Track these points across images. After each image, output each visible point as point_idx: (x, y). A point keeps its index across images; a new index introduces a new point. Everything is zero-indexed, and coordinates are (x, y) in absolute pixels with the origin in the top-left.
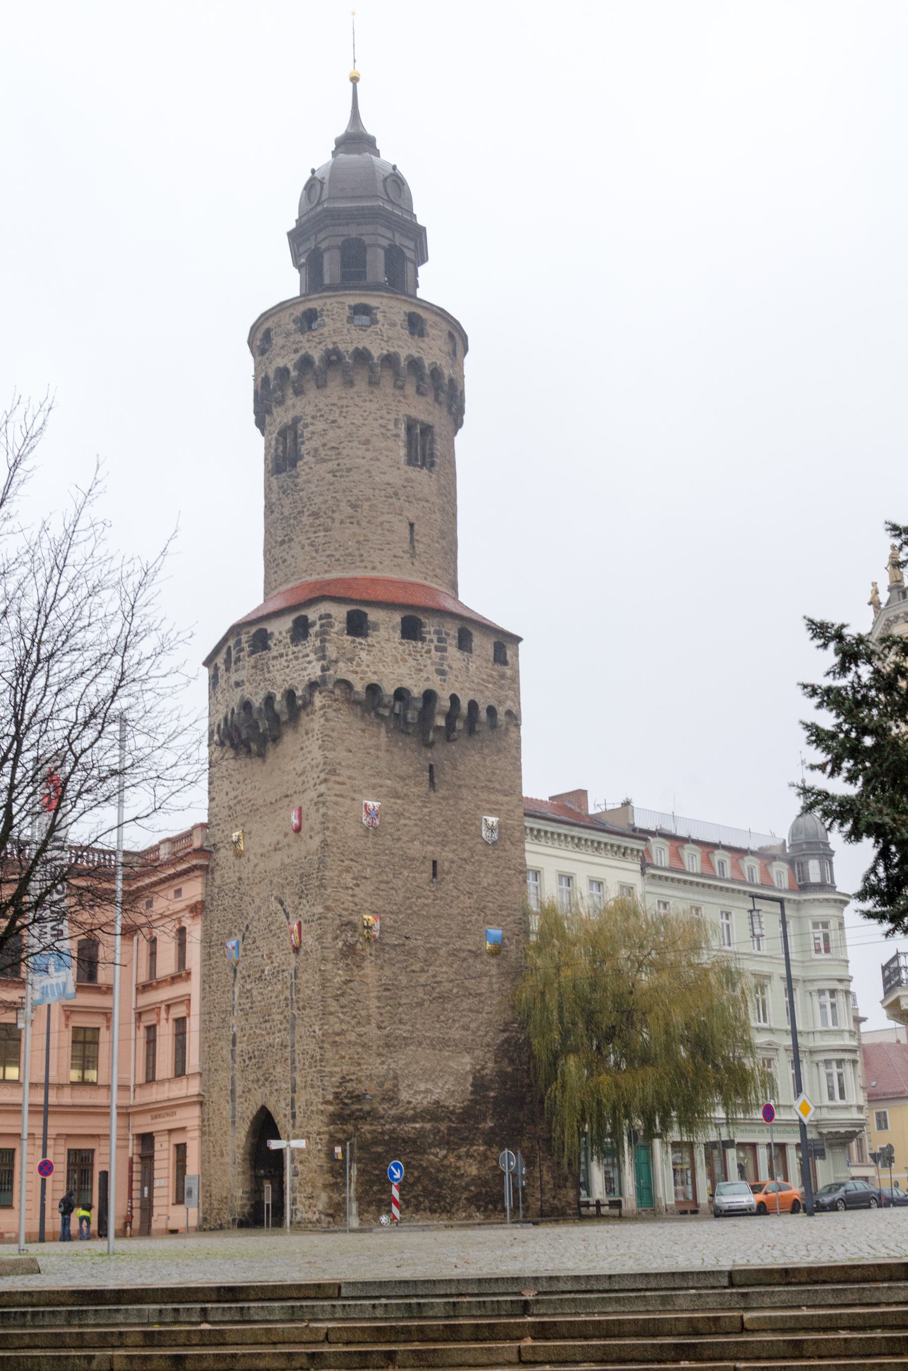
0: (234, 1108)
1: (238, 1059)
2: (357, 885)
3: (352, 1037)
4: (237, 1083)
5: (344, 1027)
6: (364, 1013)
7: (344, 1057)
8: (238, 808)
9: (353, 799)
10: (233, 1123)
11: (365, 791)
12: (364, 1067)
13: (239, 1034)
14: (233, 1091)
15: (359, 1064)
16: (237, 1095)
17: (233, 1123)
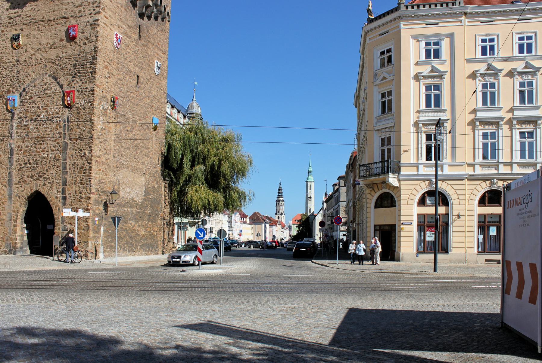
0: (11, 190)
1: (15, 163)
2: (110, 78)
3: (104, 159)
4: (14, 177)
5: (101, 153)
6: (109, 148)
7: (100, 170)
8: (17, 19)
9: (111, 29)
10: (10, 198)
11: (115, 27)
12: (108, 176)
13: (16, 149)
14: (10, 181)
15: (106, 175)
16: (13, 183)
17: (10, 198)
